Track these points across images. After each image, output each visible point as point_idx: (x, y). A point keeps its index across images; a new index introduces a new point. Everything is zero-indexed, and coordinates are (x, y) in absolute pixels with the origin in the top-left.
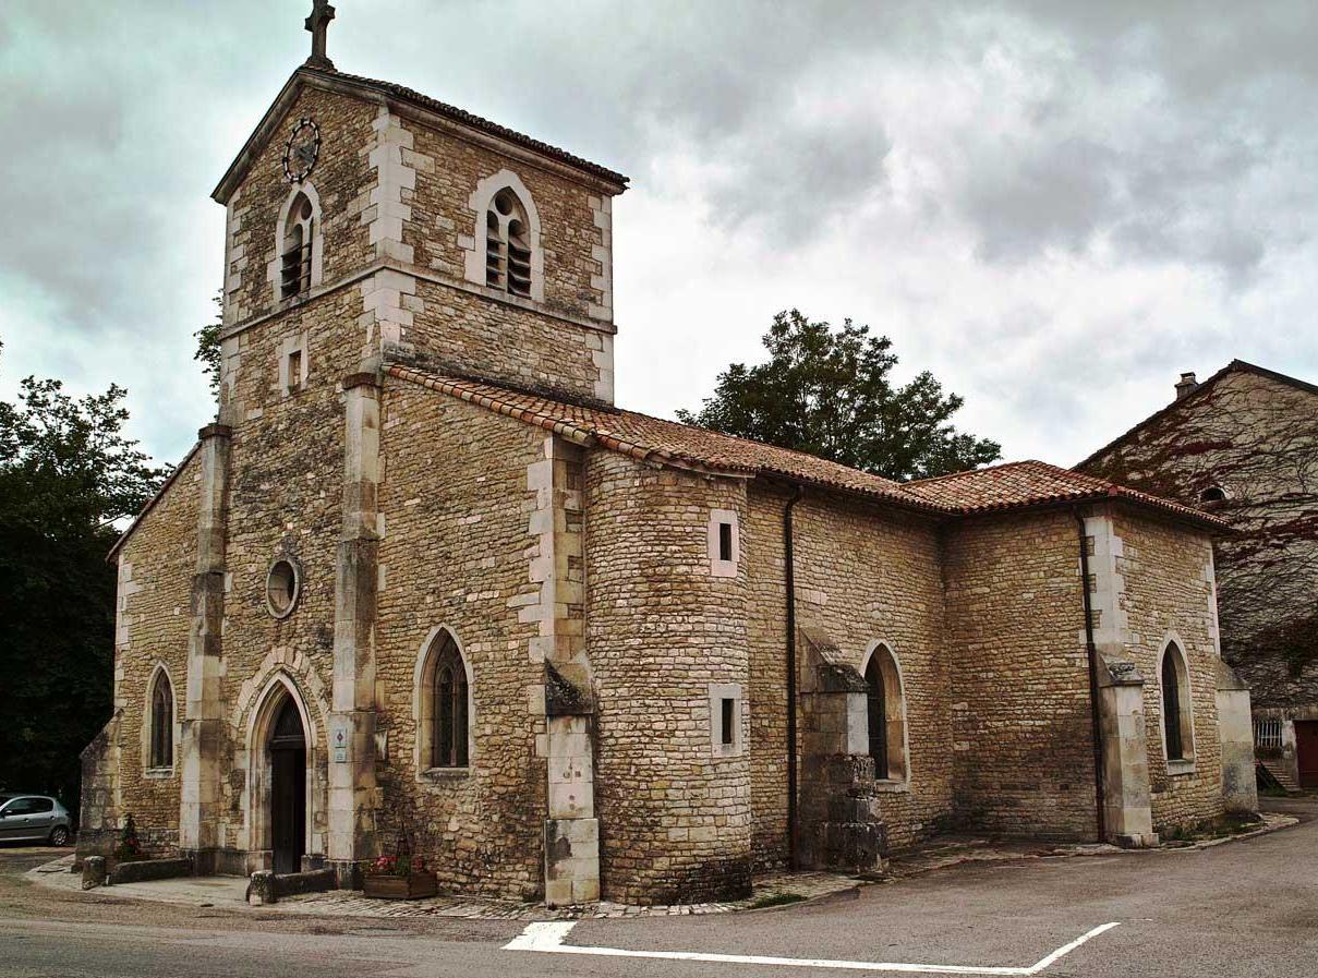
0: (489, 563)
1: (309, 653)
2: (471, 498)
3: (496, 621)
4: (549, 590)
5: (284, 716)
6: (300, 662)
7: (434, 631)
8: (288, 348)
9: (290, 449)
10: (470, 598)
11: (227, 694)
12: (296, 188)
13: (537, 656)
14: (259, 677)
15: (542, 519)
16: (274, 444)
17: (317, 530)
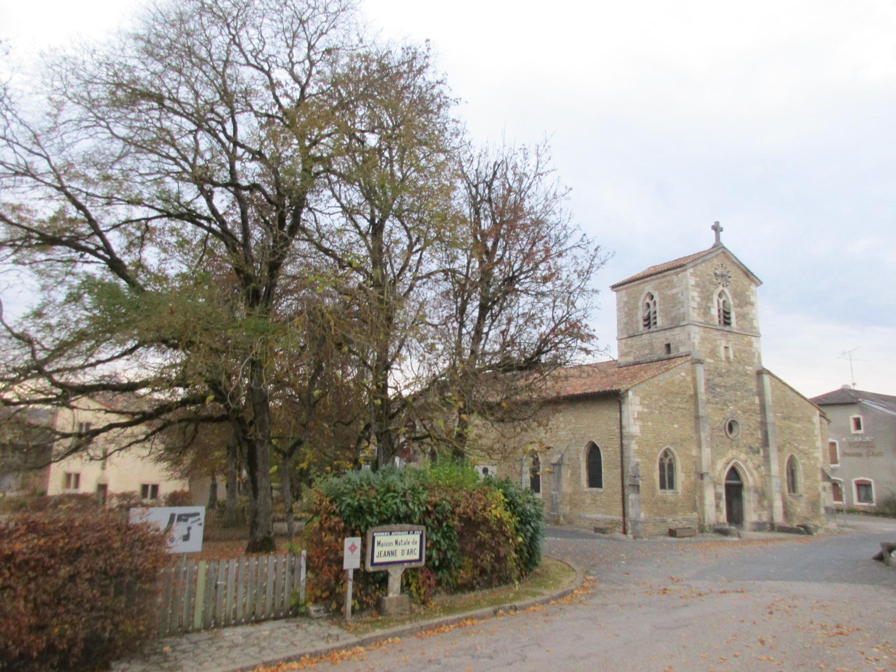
0: (804, 438)
1: (747, 454)
2: (799, 420)
3: (807, 454)
4: (820, 450)
5: (734, 473)
6: (743, 456)
7: (789, 454)
8: (723, 343)
9: (730, 381)
10: (801, 447)
11: (713, 463)
12: (721, 288)
13: (819, 466)
14: (724, 460)
15: (817, 432)
16: (721, 376)
17: (744, 412)
